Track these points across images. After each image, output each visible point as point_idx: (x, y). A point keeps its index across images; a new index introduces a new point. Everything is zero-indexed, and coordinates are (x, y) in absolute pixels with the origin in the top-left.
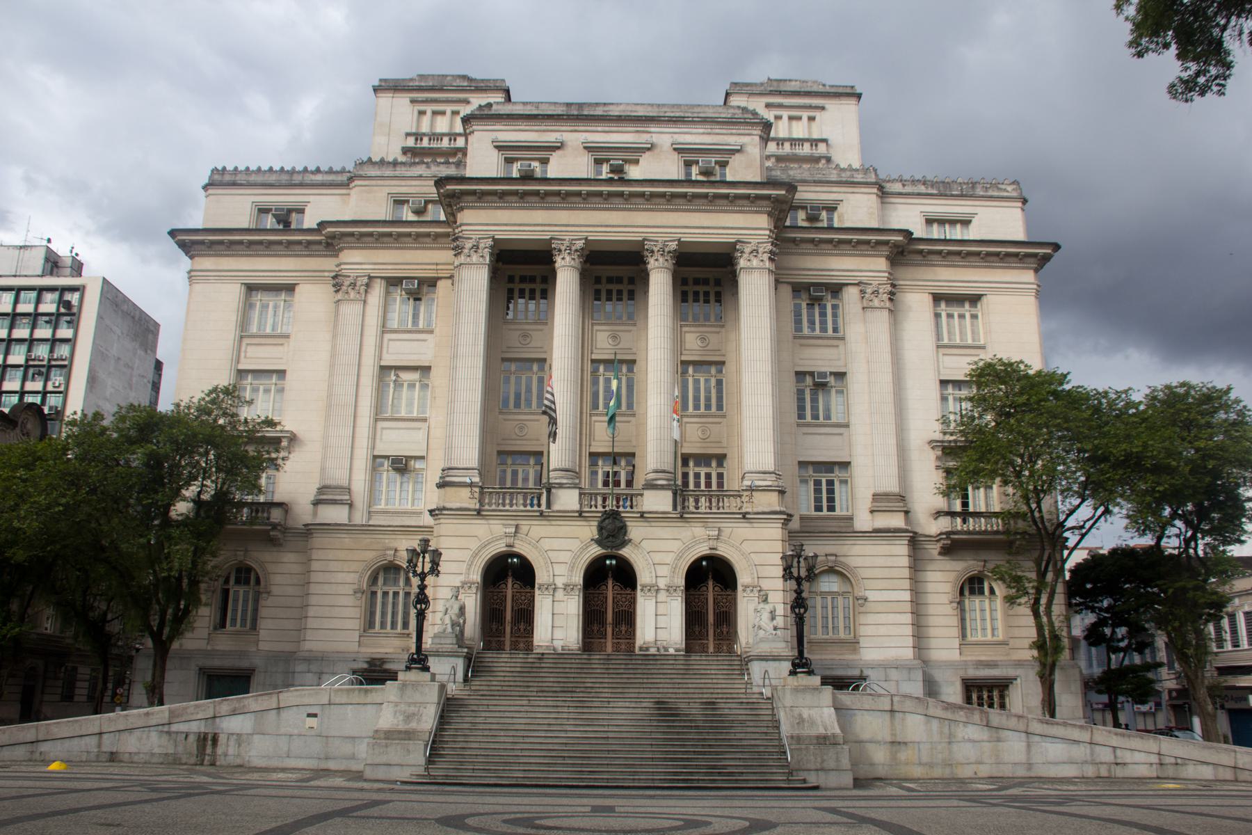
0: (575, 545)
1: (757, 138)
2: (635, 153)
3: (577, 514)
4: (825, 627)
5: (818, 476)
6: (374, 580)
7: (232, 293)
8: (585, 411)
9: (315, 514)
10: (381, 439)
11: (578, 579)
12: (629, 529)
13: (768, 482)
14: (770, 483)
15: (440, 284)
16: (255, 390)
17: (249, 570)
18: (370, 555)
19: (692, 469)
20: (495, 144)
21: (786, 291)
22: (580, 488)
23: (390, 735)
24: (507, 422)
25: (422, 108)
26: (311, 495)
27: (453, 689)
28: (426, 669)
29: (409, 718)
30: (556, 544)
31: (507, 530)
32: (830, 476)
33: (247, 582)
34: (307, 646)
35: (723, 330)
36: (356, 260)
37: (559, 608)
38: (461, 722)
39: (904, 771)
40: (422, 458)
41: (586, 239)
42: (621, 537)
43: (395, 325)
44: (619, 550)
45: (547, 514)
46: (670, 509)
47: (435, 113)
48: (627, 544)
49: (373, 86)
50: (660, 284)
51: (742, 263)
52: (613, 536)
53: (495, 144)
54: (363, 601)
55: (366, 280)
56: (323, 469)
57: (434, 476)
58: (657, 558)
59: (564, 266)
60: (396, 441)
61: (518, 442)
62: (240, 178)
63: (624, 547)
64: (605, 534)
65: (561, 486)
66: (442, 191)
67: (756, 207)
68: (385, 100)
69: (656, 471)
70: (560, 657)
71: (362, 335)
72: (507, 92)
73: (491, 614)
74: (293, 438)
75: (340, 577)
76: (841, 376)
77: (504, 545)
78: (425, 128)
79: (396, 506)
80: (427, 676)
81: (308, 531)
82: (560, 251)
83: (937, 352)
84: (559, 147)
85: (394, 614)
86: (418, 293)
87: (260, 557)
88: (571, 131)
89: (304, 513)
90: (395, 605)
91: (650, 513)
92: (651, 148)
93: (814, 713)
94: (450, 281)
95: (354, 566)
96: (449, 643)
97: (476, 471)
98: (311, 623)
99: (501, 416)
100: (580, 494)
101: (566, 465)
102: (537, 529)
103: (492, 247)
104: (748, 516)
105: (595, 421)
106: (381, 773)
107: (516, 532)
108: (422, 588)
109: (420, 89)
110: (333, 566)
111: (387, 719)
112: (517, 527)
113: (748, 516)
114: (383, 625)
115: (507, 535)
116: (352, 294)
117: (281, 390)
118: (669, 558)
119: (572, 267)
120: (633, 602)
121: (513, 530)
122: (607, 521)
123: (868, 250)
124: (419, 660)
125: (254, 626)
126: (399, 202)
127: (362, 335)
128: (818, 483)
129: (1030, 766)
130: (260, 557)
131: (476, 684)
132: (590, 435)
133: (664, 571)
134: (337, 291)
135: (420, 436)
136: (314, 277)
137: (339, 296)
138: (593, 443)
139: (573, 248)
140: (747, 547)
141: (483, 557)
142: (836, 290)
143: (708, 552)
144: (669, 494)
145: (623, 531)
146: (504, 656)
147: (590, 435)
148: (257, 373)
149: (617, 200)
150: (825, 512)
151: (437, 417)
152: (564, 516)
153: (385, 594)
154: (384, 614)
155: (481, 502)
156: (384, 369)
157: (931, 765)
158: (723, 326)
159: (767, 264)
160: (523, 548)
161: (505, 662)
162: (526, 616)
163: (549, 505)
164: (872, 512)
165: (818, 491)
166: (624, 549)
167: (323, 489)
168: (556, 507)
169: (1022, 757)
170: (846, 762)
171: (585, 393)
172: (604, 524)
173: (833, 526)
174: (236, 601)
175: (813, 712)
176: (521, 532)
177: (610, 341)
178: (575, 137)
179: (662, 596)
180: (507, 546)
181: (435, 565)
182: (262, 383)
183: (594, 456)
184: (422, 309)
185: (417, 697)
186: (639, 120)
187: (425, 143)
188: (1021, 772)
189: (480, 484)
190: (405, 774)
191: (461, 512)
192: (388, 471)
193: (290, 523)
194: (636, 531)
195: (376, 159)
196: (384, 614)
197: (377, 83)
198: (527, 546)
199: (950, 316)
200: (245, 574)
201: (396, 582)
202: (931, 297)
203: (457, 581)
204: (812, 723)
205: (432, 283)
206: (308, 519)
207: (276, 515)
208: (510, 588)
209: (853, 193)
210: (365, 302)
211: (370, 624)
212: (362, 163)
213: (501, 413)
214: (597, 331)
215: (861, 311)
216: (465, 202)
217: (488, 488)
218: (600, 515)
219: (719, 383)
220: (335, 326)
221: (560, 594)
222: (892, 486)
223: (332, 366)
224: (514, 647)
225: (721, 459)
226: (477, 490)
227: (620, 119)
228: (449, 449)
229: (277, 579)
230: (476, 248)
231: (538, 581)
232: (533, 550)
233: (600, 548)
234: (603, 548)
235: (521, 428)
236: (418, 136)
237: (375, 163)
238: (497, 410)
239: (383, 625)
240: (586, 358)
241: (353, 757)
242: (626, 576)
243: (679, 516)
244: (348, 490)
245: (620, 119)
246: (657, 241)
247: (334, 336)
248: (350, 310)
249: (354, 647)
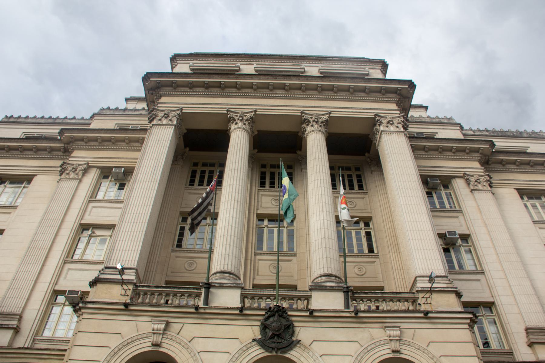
0: (234, 347)
1: (379, 71)
3: (237, 312)
8: (250, 250)
10: (65, 278)
12: (297, 330)
14: (445, 285)
20: (191, 67)
22: (242, 288)
24: (177, 259)
30: (211, 344)
31: (156, 326)
35: (367, 196)
41: (256, 111)
42: (288, 336)
44: (285, 352)
45: (202, 311)
48: (295, 346)
49: (125, 98)
52: (279, 336)
53: (191, 67)
59: (237, 128)
61: (186, 275)
63: (291, 349)
64: (270, 333)
65: (222, 286)
66: (147, 84)
67: (387, 98)
69: (324, 275)
71: (71, 202)
76: (465, 238)
77: (150, 344)
82: (235, 120)
86: (124, 180)
88: (247, 64)
91: (320, 311)
97: (134, 271)
99: (173, 254)
100: (242, 295)
104: (430, 315)
105: (260, 260)
107: (165, 329)
112: (168, 324)
113: (430, 315)
115: (155, 332)
119: (243, 129)
121: (162, 326)
122: (271, 319)
123: (465, 156)
127: (71, 202)
132: (254, 271)
138: (257, 277)
139: (245, 118)
141: (122, 357)
143: (391, 356)
145: (291, 330)
147: (254, 271)
149: (280, 92)
158: (366, 194)
160: (172, 348)
163: (206, 302)
166: (292, 352)
171: (251, 236)
172: (268, 322)
176: (172, 329)
177: (273, 202)
180: (153, 345)
186: (295, 59)
189: (135, 281)
192: (64, 305)
198: (177, 345)
202: (515, 192)
209: (444, 129)
210: (80, 181)
213: (173, 251)
214: (262, 195)
215: (470, 193)
216: (163, 91)
217: (143, 286)
218: (263, 313)
219: (368, 234)
226: (131, 287)
230: (167, 116)
232: (184, 350)
233: (262, 351)
234: (267, 351)
235: (191, 264)
238: (171, 248)
240: (252, 211)
243: (353, 315)
246: (312, 115)
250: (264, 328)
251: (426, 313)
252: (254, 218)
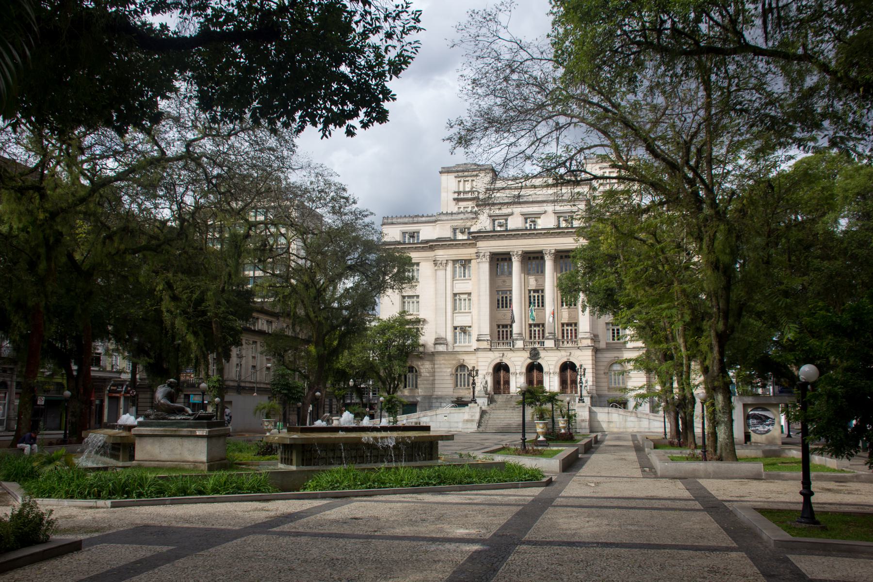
0: (523, 359)
2: (538, 215)
4: (615, 383)
5: (614, 327)
6: (457, 370)
9: (435, 348)
11: (524, 370)
13: (588, 335)
15: (472, 261)
16: (409, 303)
17: (413, 367)
18: (454, 362)
19: (565, 328)
23: (467, 421)
25: (459, 179)
26: (433, 341)
27: (484, 408)
28: (476, 403)
29: (472, 416)
30: (516, 359)
32: (618, 327)
33: (412, 372)
34: (436, 393)
36: (442, 254)
37: (518, 380)
38: (486, 417)
39: (612, 430)
40: (470, 327)
43: (457, 278)
46: (553, 346)
47: (465, 181)
50: (549, 265)
54: (454, 377)
56: (436, 332)
57: (474, 337)
58: (549, 363)
60: (461, 321)
62: (394, 221)
68: (444, 177)
73: (496, 382)
74: (424, 321)
75: (445, 370)
78: (461, 189)
79: (463, 344)
80: (476, 405)
81: (433, 354)
84: (512, 214)
85: (464, 381)
87: (416, 363)
89: (431, 348)
90: (464, 378)
92: (545, 212)
93: (583, 413)
95: (449, 366)
96: (483, 394)
98: (437, 386)
101: (518, 332)
102: (509, 354)
106: (466, 431)
108: (474, 380)
109: (458, 172)
110: (443, 366)
111: (466, 417)
114: (461, 386)
116: (441, 267)
117: (418, 302)
118: (554, 363)
120: (543, 377)
124: (474, 401)
125: (416, 387)
126: (455, 230)
128: (613, 330)
129: (649, 428)
130: (416, 363)
131: (491, 405)
133: (552, 367)
135: (469, 318)
136: (426, 259)
137: (436, 268)
140: (580, 358)
144: (553, 341)
146: (500, 396)
148: (409, 297)
150: (616, 341)
151: (474, 310)
152: (519, 350)
153: (461, 375)
154: (461, 382)
155: (491, 346)
156: (455, 295)
157: (620, 428)
161: (500, 398)
162: (507, 383)
165: (613, 333)
167: (436, 339)
168: (516, 347)
169: (647, 426)
170: (587, 426)
173: (618, 346)
174: (409, 378)
175: (583, 413)
178: (518, 210)
179: (552, 375)
181: (477, 373)
182: (411, 300)
184: (467, 271)
185: (474, 411)
187: (462, 196)
188: (647, 430)
190: (472, 430)
191: (485, 349)
193: (426, 351)
194: (542, 354)
195: (445, 212)
196: (461, 382)
200: (411, 369)
201: (464, 371)
203: (485, 372)
204: (582, 416)
206: (433, 350)
207: (421, 349)
208: (502, 373)
211: (457, 385)
212: (440, 214)
220: (436, 279)
221: (518, 375)
223: (436, 294)
224: (504, 393)
225: (576, 324)
227: (533, 202)
228: (479, 327)
229: (422, 371)
231: (511, 371)
236: (459, 193)
237: (444, 214)
239: (461, 386)
241: (457, 427)
242: (540, 368)
244: (446, 339)
245: (533, 202)
247: (436, 283)
248: (441, 273)
249: (451, 393)
251: (578, 348)
252: (527, 292)
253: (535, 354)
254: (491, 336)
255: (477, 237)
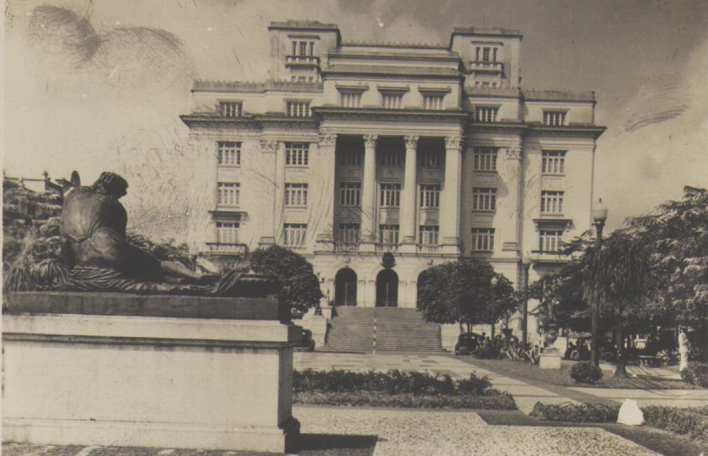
7: (213, 148)
15: (312, 146)
21: (470, 152)
36: (271, 134)
51: (447, 146)
55: (276, 143)
60: (294, 217)
70: (366, 310)
72: (337, 31)
83: (542, 178)
94: (315, 145)
103: (337, 138)
116: (270, 150)
134: (263, 148)
137: (264, 150)
142: (496, 149)
159: (458, 147)
164: (503, 250)
182: (229, 188)
183: (382, 227)
194: (398, 260)
197: (270, 26)
199: (551, 160)
205: (307, 145)
210: (276, 153)
222: (513, 239)
230: (329, 139)
250: (383, 260)
253: (389, 260)
254: (334, 237)
255: (321, 115)
